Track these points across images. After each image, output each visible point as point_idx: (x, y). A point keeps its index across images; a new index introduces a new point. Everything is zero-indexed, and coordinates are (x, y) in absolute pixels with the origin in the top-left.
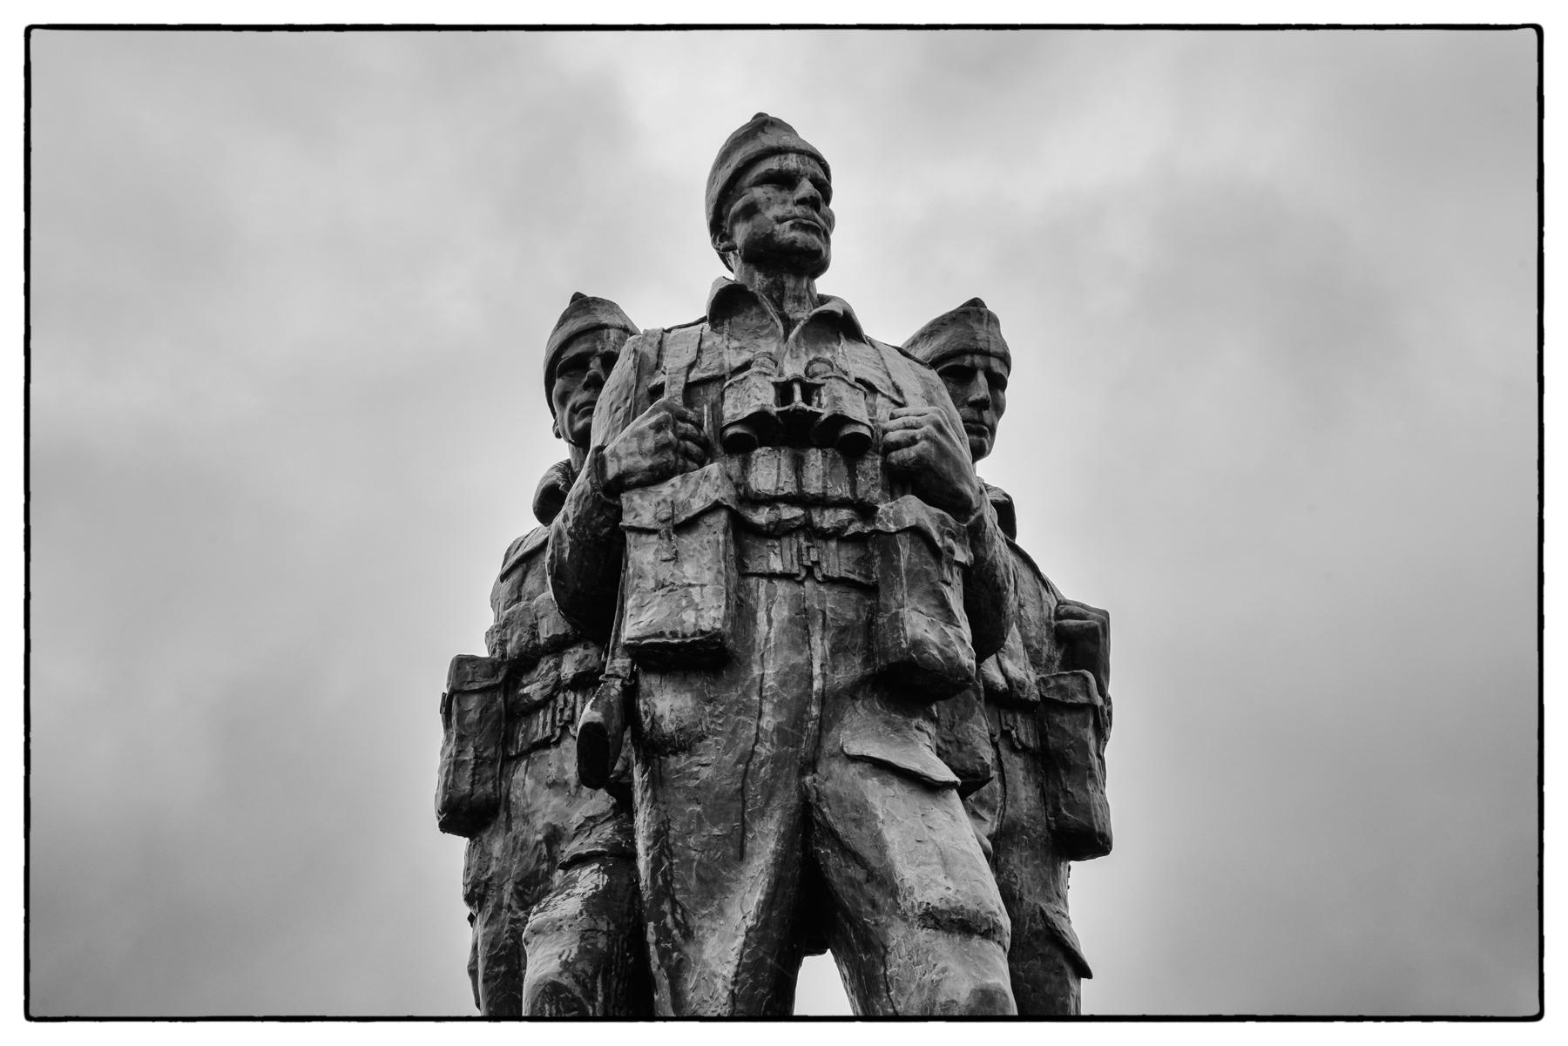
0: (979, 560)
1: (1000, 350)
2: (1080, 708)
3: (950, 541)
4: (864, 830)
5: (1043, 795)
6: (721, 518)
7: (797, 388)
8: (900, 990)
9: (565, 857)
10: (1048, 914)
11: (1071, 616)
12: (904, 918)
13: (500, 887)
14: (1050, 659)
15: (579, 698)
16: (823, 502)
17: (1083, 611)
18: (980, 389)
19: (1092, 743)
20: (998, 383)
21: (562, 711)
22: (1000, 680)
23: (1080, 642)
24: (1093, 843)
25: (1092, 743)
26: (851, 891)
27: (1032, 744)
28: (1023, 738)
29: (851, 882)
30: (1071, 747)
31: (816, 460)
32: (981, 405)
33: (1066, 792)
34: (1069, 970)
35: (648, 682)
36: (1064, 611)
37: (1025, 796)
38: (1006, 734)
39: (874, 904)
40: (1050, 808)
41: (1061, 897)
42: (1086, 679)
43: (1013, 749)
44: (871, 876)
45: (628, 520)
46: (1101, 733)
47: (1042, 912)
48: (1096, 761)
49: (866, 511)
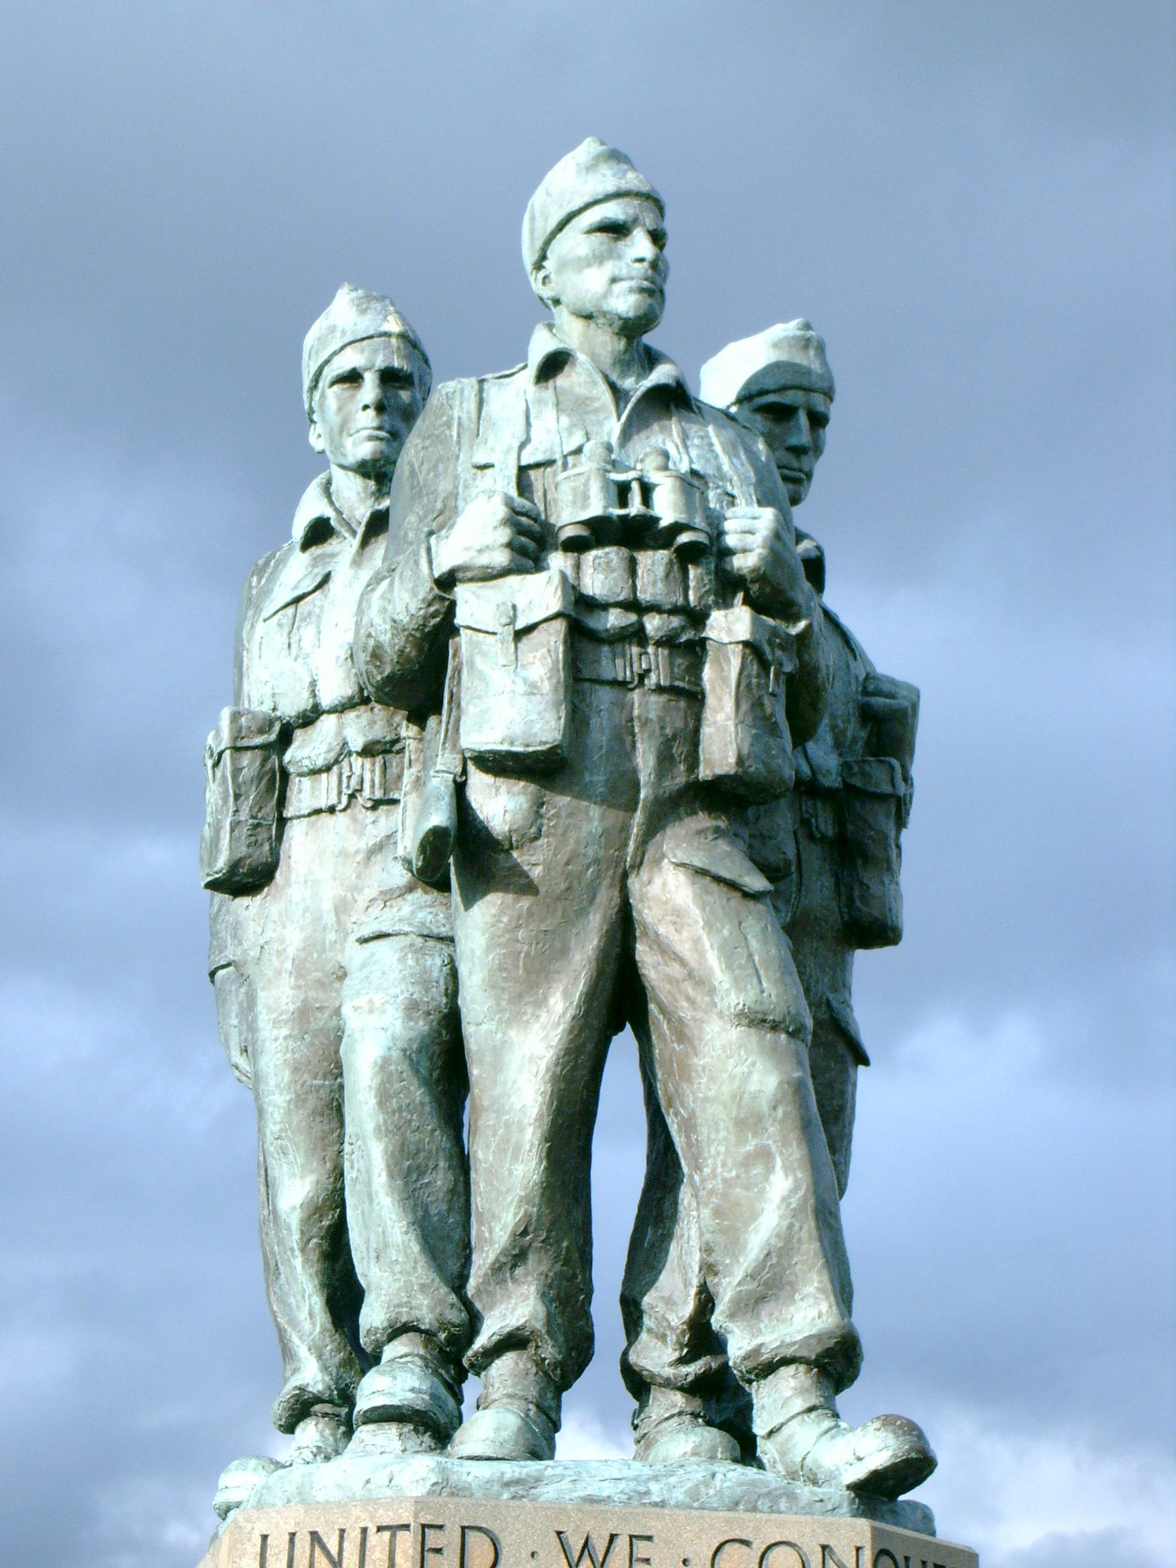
0: (803, 665)
1: (825, 385)
2: (883, 798)
3: (779, 653)
4: (685, 934)
5: (837, 884)
6: (560, 626)
7: (635, 486)
8: (712, 1079)
9: (366, 932)
10: (834, 1004)
11: (879, 693)
12: (721, 1015)
14: (854, 740)
15: (368, 765)
16: (654, 608)
17: (893, 689)
18: (802, 434)
19: (893, 834)
20: (818, 420)
21: (349, 777)
22: (805, 769)
23: (886, 725)
24: (880, 932)
25: (893, 834)
26: (668, 986)
27: (830, 833)
28: (822, 827)
29: (670, 979)
30: (871, 837)
31: (653, 563)
32: (798, 451)
33: (862, 883)
34: (849, 1058)
36: (871, 685)
37: (820, 890)
38: (805, 823)
39: (691, 1001)
40: (843, 898)
41: (846, 986)
42: (892, 768)
43: (811, 837)
44: (690, 975)
46: (901, 821)
47: (828, 1003)
48: (895, 851)
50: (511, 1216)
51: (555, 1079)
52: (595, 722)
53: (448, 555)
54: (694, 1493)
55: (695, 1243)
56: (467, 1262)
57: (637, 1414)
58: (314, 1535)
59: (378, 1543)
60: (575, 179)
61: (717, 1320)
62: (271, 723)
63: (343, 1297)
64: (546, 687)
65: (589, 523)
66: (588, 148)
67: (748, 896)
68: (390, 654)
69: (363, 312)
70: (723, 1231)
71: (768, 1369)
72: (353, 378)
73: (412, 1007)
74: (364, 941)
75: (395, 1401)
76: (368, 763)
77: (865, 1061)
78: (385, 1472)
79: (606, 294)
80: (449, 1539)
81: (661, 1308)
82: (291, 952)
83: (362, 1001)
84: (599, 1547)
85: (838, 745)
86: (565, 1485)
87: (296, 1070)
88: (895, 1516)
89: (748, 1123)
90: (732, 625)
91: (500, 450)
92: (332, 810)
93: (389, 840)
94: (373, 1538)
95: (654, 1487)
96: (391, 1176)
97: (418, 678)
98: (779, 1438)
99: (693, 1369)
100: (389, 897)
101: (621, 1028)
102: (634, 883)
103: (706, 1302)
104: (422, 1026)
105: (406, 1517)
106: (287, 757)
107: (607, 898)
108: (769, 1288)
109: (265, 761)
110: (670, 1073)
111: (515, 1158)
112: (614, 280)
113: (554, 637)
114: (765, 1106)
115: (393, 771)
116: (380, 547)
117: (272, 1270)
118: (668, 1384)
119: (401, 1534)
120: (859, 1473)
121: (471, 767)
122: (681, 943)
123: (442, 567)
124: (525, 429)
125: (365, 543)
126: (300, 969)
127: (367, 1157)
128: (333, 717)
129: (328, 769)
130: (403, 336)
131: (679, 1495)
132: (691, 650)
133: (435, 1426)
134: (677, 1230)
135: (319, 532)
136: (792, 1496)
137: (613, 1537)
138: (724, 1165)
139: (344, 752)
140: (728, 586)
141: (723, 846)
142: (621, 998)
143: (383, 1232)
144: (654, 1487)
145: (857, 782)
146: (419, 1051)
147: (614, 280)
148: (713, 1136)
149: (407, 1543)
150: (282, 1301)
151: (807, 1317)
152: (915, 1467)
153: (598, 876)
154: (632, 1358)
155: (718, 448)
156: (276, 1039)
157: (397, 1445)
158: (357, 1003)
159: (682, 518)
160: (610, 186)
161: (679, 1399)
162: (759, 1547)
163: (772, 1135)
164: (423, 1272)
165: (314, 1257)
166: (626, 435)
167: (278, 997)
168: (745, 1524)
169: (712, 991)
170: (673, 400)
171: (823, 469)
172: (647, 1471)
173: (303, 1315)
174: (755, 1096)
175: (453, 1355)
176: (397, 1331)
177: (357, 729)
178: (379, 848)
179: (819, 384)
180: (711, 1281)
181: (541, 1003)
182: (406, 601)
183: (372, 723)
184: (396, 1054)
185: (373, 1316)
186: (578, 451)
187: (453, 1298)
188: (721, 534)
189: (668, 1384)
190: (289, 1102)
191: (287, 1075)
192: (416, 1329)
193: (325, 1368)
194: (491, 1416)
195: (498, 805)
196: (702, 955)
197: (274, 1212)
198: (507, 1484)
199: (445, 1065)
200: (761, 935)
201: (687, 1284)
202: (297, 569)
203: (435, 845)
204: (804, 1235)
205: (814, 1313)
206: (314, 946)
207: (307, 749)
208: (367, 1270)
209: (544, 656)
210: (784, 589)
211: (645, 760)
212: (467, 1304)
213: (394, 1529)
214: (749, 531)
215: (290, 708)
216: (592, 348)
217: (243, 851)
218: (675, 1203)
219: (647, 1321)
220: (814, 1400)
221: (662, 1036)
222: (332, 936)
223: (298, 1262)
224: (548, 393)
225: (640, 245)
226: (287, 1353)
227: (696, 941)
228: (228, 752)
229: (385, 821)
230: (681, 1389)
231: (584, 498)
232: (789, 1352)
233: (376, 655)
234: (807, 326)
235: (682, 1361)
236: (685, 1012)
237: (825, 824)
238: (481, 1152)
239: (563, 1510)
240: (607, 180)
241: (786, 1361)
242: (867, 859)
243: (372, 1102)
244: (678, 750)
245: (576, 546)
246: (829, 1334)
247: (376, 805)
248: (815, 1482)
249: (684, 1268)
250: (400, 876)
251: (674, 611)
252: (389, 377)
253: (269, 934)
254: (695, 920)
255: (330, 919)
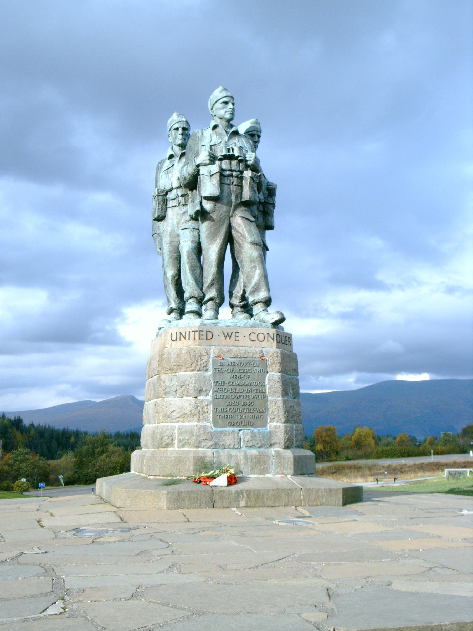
2: (271, 204)
5: (264, 219)
6: (218, 174)
8: (246, 254)
9: (183, 228)
16: (234, 171)
18: (256, 138)
20: (259, 137)
23: (271, 191)
24: (270, 227)
29: (238, 236)
31: (234, 163)
32: (256, 142)
35: (204, 202)
36: (268, 184)
37: (261, 220)
38: (258, 208)
39: (242, 240)
43: (259, 211)
44: (242, 235)
45: (201, 172)
46: (274, 208)
49: (242, 172)
51: (218, 254)
52: (224, 191)
53: (198, 161)
54: (245, 325)
55: (242, 282)
56: (203, 285)
57: (232, 311)
58: (180, 333)
59: (192, 334)
60: (218, 93)
61: (246, 295)
62: (164, 191)
63: (180, 292)
64: (216, 185)
65: (223, 156)
66: (220, 88)
67: (251, 221)
68: (187, 179)
69: (179, 117)
70: (248, 280)
71: (256, 303)
72: (177, 129)
73: (192, 241)
74: (182, 229)
75: (192, 310)
76: (182, 198)
77: (268, 250)
78: (189, 321)
79: (225, 114)
80: (204, 333)
81: (236, 293)
82: (169, 231)
83: (184, 240)
84: (230, 334)
85: (263, 194)
86: (223, 324)
87: (170, 252)
88: (278, 328)
89: (252, 261)
90: (248, 174)
91: (207, 142)
92: (176, 206)
93: (186, 212)
94: (191, 333)
95: (238, 324)
96: (190, 271)
97: (192, 183)
98: (258, 315)
99: (242, 304)
100: (186, 222)
101: (227, 244)
102: (231, 219)
103: (244, 292)
104: (194, 244)
105: (197, 329)
106: (167, 197)
107: (227, 222)
108: (256, 290)
109: (163, 197)
110: (238, 253)
111: (211, 267)
112: (226, 112)
113: (218, 176)
114: (255, 258)
115: (187, 199)
116: (183, 160)
117: (166, 287)
118: (238, 306)
119: (196, 332)
120: (273, 321)
121: (203, 199)
122: (240, 230)
123: (197, 163)
124: (209, 139)
125: (180, 158)
126: (170, 234)
127: (185, 267)
128: (175, 190)
129: (175, 199)
130: (186, 121)
131: (242, 325)
132: (241, 178)
133: (199, 314)
134: (239, 280)
135: (171, 157)
136: (261, 325)
137: (232, 332)
139: (178, 196)
140: (247, 167)
141: (247, 213)
142: (229, 239)
144: (238, 324)
145: (267, 201)
146: (194, 249)
147: (226, 112)
149: (197, 334)
150: (168, 292)
151: (262, 295)
152: (282, 320)
153: (225, 218)
154: (231, 302)
155: (244, 142)
157: (193, 317)
158: (184, 240)
159: (239, 155)
160: (225, 95)
161: (239, 309)
162: (257, 334)
163: (256, 264)
164: (196, 287)
165: (174, 285)
166: (229, 140)
167: (166, 239)
168: (255, 330)
169: (246, 238)
170: (236, 133)
171: (260, 145)
172: (237, 321)
173: (172, 295)
174: (253, 256)
175: (200, 301)
176: (191, 297)
177: (180, 192)
178: (184, 213)
179: (259, 130)
180: (245, 288)
181: (215, 240)
182: (190, 170)
183: (182, 191)
184: (190, 249)
185: (186, 295)
186: (220, 142)
187: (201, 292)
188: (245, 158)
189: (238, 306)
191: (168, 253)
192: (194, 297)
193: (176, 304)
194: (208, 312)
195: (208, 206)
196: (244, 232)
197: (166, 277)
198: (213, 324)
199: (198, 250)
200: (253, 228)
201: (241, 289)
202: (167, 164)
203: (197, 213)
204: (262, 280)
205: (264, 294)
206: (172, 230)
207: (171, 195)
208: (185, 287)
209: (216, 180)
210: (255, 168)
211: (233, 198)
212: (203, 292)
213: (195, 331)
214: (250, 157)
215: (168, 188)
216: (222, 124)
217: (160, 214)
218: (238, 275)
219: (234, 295)
220: (264, 309)
221: (236, 246)
223: (171, 285)
224: (214, 132)
225: (230, 106)
226: (169, 301)
227: (243, 229)
228: (157, 197)
229: (185, 209)
230: (240, 307)
231: (222, 152)
232: (260, 301)
233: (185, 179)
234: (257, 120)
235: (240, 302)
236: (241, 242)
237: (262, 209)
238: (205, 267)
239: (224, 328)
240: (224, 94)
241: (259, 302)
242: (269, 215)
243: (186, 258)
244: (239, 196)
245: (221, 160)
246: (267, 297)
247: (184, 205)
248: (265, 323)
249: (240, 286)
250: (188, 218)
251: (238, 171)
252: (184, 129)
253: (165, 228)
254: (242, 225)
255: (176, 226)
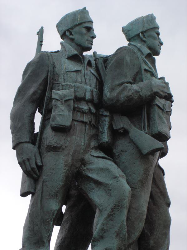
13: (70, 150)
50: (137, 234)
138: (159, 234)
143: (121, 230)
148: (159, 227)
156: (65, 169)
190: (63, 185)
222: (82, 151)
